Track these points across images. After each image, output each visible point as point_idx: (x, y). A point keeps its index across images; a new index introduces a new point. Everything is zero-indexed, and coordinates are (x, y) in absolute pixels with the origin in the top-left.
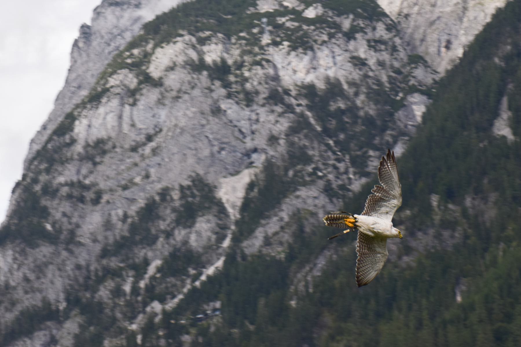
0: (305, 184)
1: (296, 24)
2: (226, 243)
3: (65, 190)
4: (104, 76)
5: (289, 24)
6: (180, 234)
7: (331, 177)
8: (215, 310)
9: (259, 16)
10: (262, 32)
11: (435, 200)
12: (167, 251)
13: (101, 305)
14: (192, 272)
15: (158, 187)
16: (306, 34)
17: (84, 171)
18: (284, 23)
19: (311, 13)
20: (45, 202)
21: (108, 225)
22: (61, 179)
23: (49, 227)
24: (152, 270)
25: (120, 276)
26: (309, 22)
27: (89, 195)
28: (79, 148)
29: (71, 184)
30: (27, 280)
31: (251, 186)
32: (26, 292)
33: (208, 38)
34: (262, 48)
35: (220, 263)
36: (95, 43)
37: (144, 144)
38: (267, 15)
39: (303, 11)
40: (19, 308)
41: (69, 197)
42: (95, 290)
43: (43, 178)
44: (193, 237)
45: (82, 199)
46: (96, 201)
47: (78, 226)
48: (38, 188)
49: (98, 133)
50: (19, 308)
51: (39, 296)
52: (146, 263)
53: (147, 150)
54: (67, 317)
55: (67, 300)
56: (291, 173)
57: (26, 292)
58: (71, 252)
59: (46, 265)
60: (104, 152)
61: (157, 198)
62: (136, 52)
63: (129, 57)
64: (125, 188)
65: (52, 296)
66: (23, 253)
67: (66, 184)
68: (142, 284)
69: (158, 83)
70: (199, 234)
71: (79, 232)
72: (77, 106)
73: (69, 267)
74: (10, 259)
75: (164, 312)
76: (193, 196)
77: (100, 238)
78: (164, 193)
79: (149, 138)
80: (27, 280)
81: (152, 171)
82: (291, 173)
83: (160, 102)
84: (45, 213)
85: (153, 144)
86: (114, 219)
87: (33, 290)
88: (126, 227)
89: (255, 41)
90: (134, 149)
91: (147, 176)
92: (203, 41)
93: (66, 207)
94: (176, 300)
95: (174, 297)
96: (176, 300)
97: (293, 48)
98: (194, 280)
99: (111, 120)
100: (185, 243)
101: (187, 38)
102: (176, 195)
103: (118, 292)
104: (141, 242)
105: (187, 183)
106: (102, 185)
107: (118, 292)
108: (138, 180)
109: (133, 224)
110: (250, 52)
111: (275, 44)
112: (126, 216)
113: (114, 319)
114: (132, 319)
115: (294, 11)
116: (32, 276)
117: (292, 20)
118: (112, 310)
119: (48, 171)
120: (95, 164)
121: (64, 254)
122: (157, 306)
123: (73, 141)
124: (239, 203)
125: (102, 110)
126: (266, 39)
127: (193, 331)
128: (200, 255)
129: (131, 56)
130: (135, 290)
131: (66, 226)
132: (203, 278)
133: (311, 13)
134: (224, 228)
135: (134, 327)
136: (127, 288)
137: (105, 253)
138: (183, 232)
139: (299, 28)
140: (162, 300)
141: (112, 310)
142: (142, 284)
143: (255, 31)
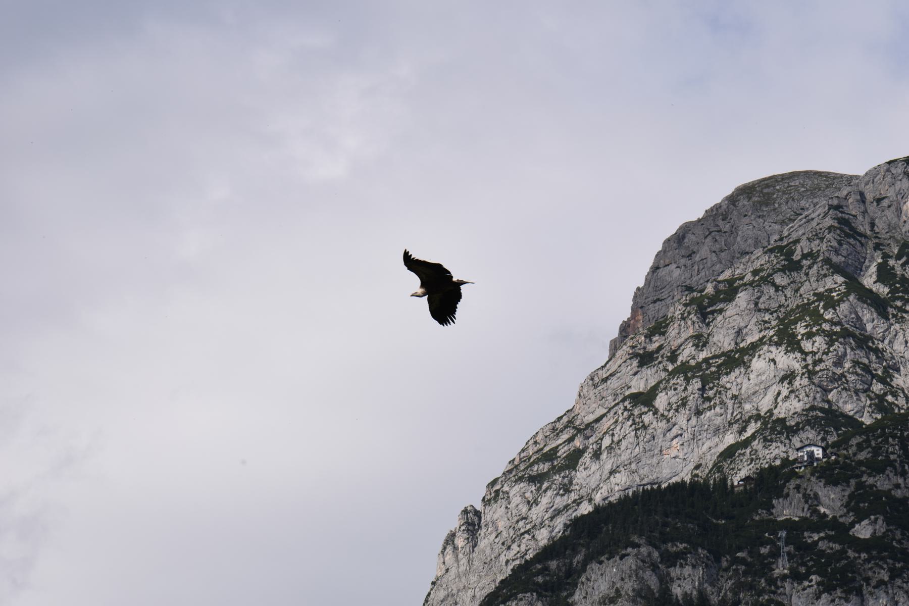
1: (837, 547)
5: (822, 545)
9: (774, 526)
10: (775, 554)
16: (851, 566)
18: (816, 543)
19: (863, 531)
26: (861, 545)
33: (682, 555)
34: (772, 581)
38: (788, 524)
39: (852, 525)
62: (553, 564)
63: (539, 573)
89: (763, 567)
92: (671, 559)
97: (827, 587)
101: (644, 550)
110: (751, 587)
111: (796, 577)
115: (834, 524)
117: (829, 538)
126: (781, 567)
129: (545, 570)
133: (863, 531)
139: (842, 553)
143: (764, 551)
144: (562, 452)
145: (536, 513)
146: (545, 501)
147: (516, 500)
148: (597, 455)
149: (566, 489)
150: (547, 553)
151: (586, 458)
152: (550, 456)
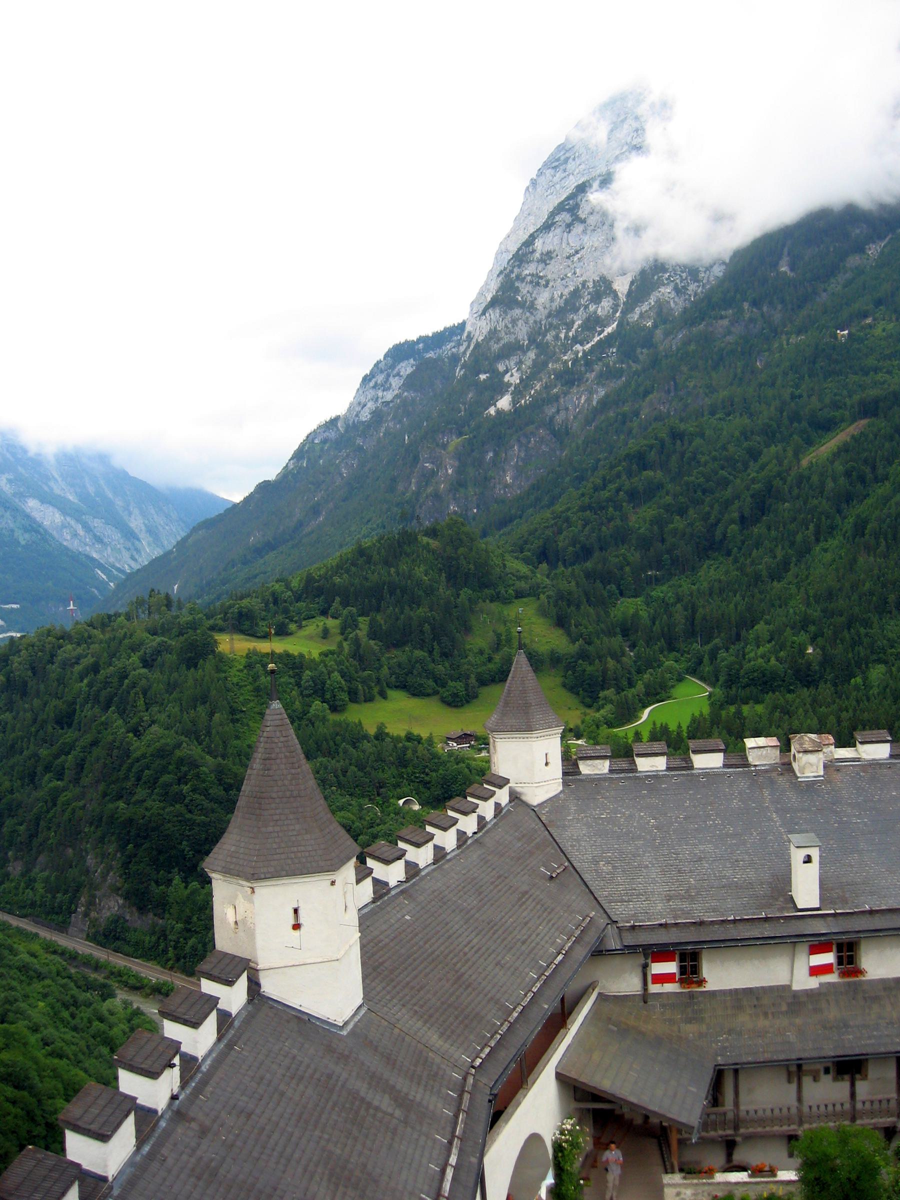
0: (664, 285)
2: (618, 314)
3: (529, 278)
4: (553, 214)
6: (592, 308)
7: (678, 281)
8: (613, 353)
11: (746, 306)
12: (585, 316)
13: (547, 343)
14: (599, 329)
15: (581, 279)
17: (540, 268)
20: (517, 284)
21: (552, 300)
22: (527, 272)
23: (520, 299)
24: (576, 326)
25: (559, 328)
27: (543, 282)
28: (537, 255)
29: (532, 275)
30: (506, 326)
31: (632, 283)
32: (506, 334)
35: (615, 325)
36: (538, 190)
37: (574, 255)
40: (502, 342)
41: (531, 282)
42: (545, 336)
43: (516, 270)
44: (600, 309)
45: (538, 284)
46: (546, 286)
47: (536, 299)
48: (513, 275)
49: (547, 248)
50: (502, 342)
51: (513, 337)
52: (573, 322)
53: (576, 259)
54: (528, 349)
55: (529, 340)
56: (656, 277)
57: (506, 334)
58: (532, 313)
59: (518, 319)
60: (551, 258)
61: (580, 286)
62: (571, 202)
64: (562, 279)
65: (520, 337)
66: (505, 312)
67: (530, 275)
68: (571, 334)
69: (583, 221)
70: (603, 308)
71: (536, 302)
72: (537, 230)
73: (531, 321)
74: (498, 315)
75: (584, 351)
76: (601, 287)
77: (548, 306)
78: (584, 284)
79: (577, 252)
80: (506, 326)
81: (578, 270)
82: (656, 277)
83: (584, 232)
84: (517, 290)
85: (579, 256)
86: (556, 296)
87: (510, 333)
88: (562, 301)
90: (568, 258)
91: (575, 273)
93: (529, 288)
94: (590, 345)
95: (588, 343)
96: (590, 345)
98: (599, 335)
99: (556, 241)
100: (595, 312)
102: (591, 284)
103: (557, 337)
104: (570, 310)
105: (597, 278)
106: (549, 277)
107: (557, 337)
108: (569, 275)
109: (566, 300)
112: (562, 295)
113: (555, 353)
114: (565, 353)
116: (510, 326)
118: (554, 347)
119: (519, 266)
120: (546, 264)
121: (528, 314)
122: (578, 347)
123: (534, 251)
124: (626, 292)
125: (551, 234)
127: (600, 364)
128: (603, 321)
130: (566, 337)
131: (529, 299)
132: (605, 333)
134: (617, 305)
135: (566, 358)
136: (562, 336)
137: (549, 315)
138: (594, 307)
140: (582, 345)
141: (554, 347)
142: (571, 334)
144: (562, 158)
145: (556, 179)
146: (558, 175)
147: (548, 175)
148: (574, 159)
149: (565, 171)
150: (568, 198)
151: (571, 160)
152: (558, 160)
